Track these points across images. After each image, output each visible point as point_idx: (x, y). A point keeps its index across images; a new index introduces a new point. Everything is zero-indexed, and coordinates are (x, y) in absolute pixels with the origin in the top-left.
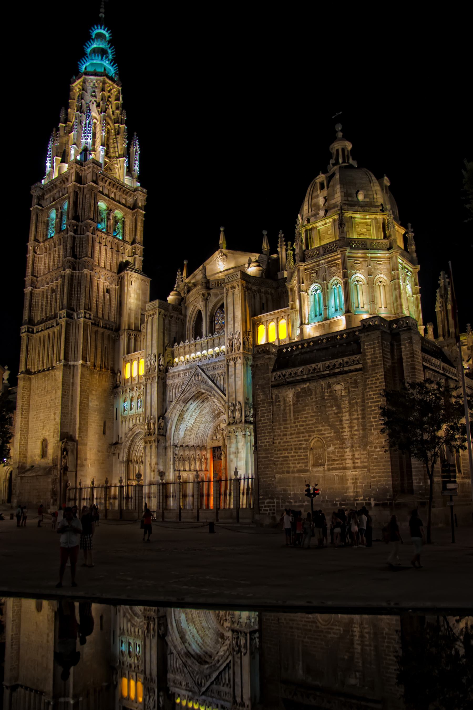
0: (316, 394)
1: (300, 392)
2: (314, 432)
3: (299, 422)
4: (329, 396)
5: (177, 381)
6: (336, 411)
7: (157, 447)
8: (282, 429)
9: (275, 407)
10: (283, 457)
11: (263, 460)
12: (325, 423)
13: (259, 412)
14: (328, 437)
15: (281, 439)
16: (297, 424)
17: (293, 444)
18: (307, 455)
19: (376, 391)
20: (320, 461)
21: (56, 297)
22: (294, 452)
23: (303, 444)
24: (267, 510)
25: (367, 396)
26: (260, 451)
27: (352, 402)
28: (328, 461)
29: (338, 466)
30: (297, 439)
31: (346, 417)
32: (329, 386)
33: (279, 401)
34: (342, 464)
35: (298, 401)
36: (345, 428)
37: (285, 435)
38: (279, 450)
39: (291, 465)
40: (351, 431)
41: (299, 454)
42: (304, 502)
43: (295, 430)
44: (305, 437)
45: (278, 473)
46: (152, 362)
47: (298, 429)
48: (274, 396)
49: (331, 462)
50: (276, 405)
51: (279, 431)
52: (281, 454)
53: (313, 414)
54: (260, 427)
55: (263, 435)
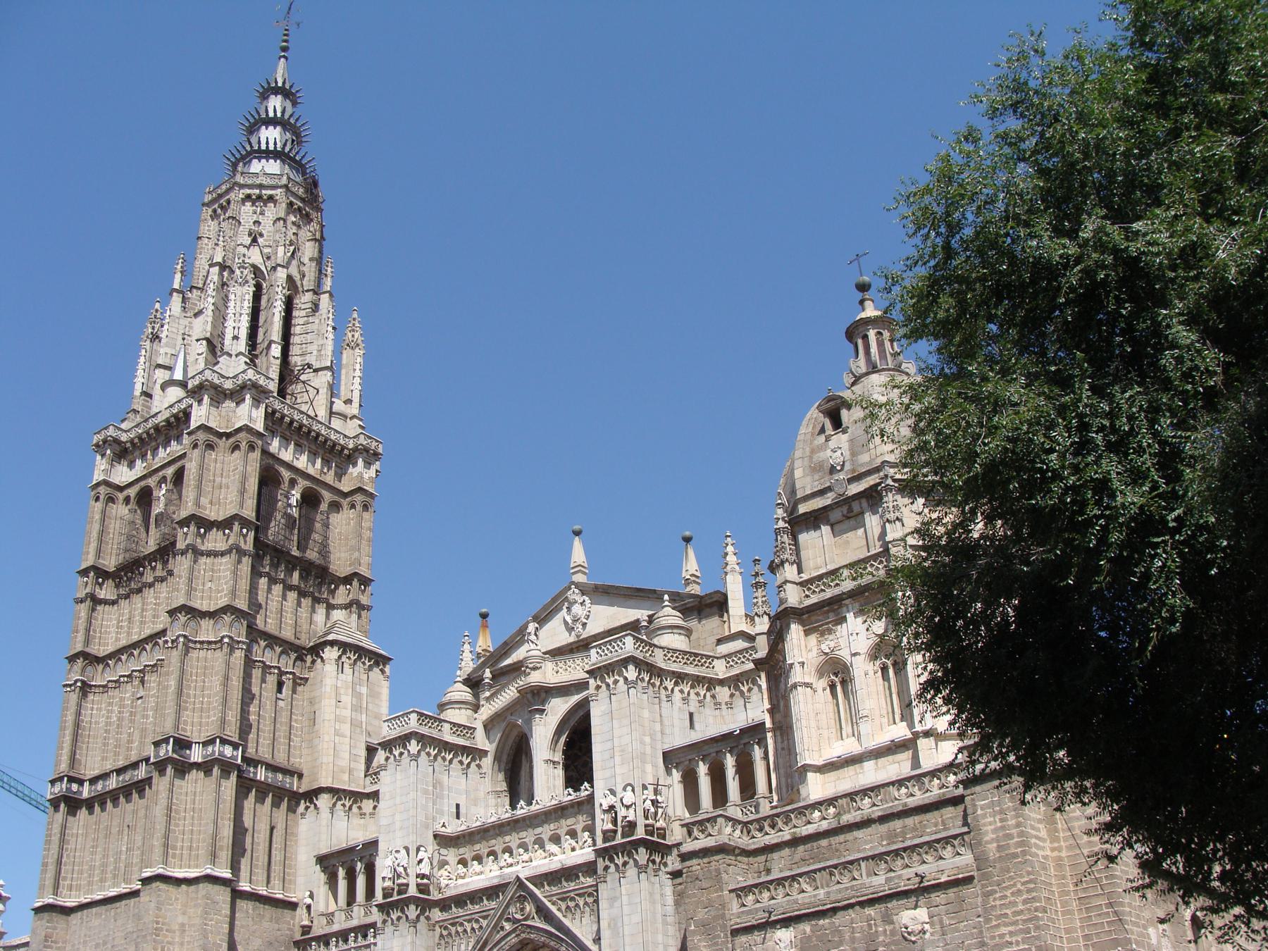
0: (853, 940)
19: (1015, 923)
25: (993, 938)
32: (887, 919)
46: (400, 870)
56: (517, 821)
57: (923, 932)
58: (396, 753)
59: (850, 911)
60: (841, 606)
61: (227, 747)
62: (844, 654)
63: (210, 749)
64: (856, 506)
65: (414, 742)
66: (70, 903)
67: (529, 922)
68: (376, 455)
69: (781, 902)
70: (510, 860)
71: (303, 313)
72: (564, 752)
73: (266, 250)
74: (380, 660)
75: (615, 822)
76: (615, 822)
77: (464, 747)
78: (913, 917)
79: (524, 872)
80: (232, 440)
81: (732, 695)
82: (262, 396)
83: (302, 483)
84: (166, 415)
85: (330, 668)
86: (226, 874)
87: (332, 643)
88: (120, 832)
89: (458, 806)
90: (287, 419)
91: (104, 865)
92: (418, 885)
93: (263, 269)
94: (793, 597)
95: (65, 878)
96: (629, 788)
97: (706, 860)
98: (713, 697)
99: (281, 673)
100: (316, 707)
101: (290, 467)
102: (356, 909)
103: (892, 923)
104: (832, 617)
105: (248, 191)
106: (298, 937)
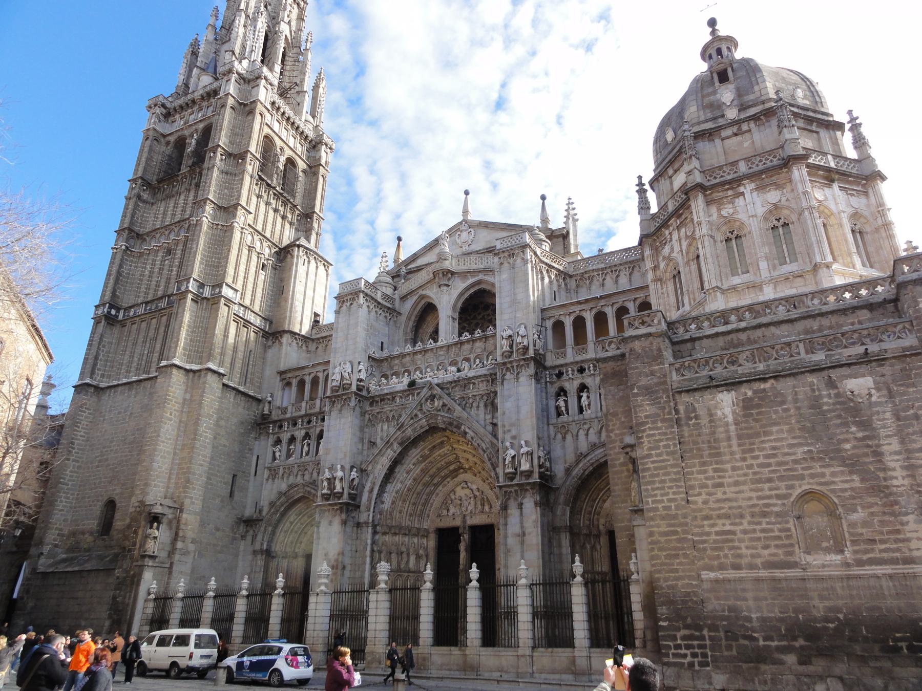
0: (796, 401)
1: (751, 399)
2: (802, 477)
3: (757, 457)
4: (834, 404)
5: (387, 408)
6: (860, 435)
7: (344, 523)
8: (711, 473)
9: (685, 428)
10: (717, 533)
11: (663, 539)
12: (831, 459)
13: (645, 439)
14: (845, 490)
15: (710, 494)
16: (750, 462)
17: (744, 504)
18: (789, 530)
20: (825, 544)
21: (172, 261)
22: (749, 523)
23: (775, 505)
24: (685, 656)
26: (652, 519)
27: (903, 414)
28: (854, 542)
29: (885, 555)
30: (754, 494)
31: (890, 446)
32: (831, 384)
33: (697, 417)
34: (898, 550)
35: (744, 416)
36: (894, 469)
37: (720, 485)
38: (707, 518)
39: (744, 551)
40: (913, 476)
41: (764, 526)
42: (795, 639)
43: (745, 475)
44: (777, 489)
45: (710, 569)
47: (755, 473)
48: (681, 408)
49: (863, 547)
50: (688, 425)
51: (702, 476)
52: (713, 526)
53: (795, 441)
54: (649, 469)
55: (657, 485)
56: (426, 351)
57: (870, 395)
58: (348, 304)
59: (792, 378)
60: (739, 186)
62: (742, 216)
63: (217, 291)
64: (745, 127)
65: (362, 295)
66: (103, 385)
69: (719, 371)
72: (460, 313)
73: (272, 14)
74: (327, 264)
76: (511, 346)
77: (389, 308)
78: (860, 384)
79: (436, 381)
80: (247, 108)
81: (577, 286)
83: (288, 153)
84: (201, 92)
86: (222, 371)
87: (299, 246)
90: (282, 110)
94: (698, 178)
95: (99, 370)
96: (523, 326)
97: (648, 342)
98: (566, 285)
102: (304, 404)
103: (836, 387)
104: (730, 193)
106: (260, 421)
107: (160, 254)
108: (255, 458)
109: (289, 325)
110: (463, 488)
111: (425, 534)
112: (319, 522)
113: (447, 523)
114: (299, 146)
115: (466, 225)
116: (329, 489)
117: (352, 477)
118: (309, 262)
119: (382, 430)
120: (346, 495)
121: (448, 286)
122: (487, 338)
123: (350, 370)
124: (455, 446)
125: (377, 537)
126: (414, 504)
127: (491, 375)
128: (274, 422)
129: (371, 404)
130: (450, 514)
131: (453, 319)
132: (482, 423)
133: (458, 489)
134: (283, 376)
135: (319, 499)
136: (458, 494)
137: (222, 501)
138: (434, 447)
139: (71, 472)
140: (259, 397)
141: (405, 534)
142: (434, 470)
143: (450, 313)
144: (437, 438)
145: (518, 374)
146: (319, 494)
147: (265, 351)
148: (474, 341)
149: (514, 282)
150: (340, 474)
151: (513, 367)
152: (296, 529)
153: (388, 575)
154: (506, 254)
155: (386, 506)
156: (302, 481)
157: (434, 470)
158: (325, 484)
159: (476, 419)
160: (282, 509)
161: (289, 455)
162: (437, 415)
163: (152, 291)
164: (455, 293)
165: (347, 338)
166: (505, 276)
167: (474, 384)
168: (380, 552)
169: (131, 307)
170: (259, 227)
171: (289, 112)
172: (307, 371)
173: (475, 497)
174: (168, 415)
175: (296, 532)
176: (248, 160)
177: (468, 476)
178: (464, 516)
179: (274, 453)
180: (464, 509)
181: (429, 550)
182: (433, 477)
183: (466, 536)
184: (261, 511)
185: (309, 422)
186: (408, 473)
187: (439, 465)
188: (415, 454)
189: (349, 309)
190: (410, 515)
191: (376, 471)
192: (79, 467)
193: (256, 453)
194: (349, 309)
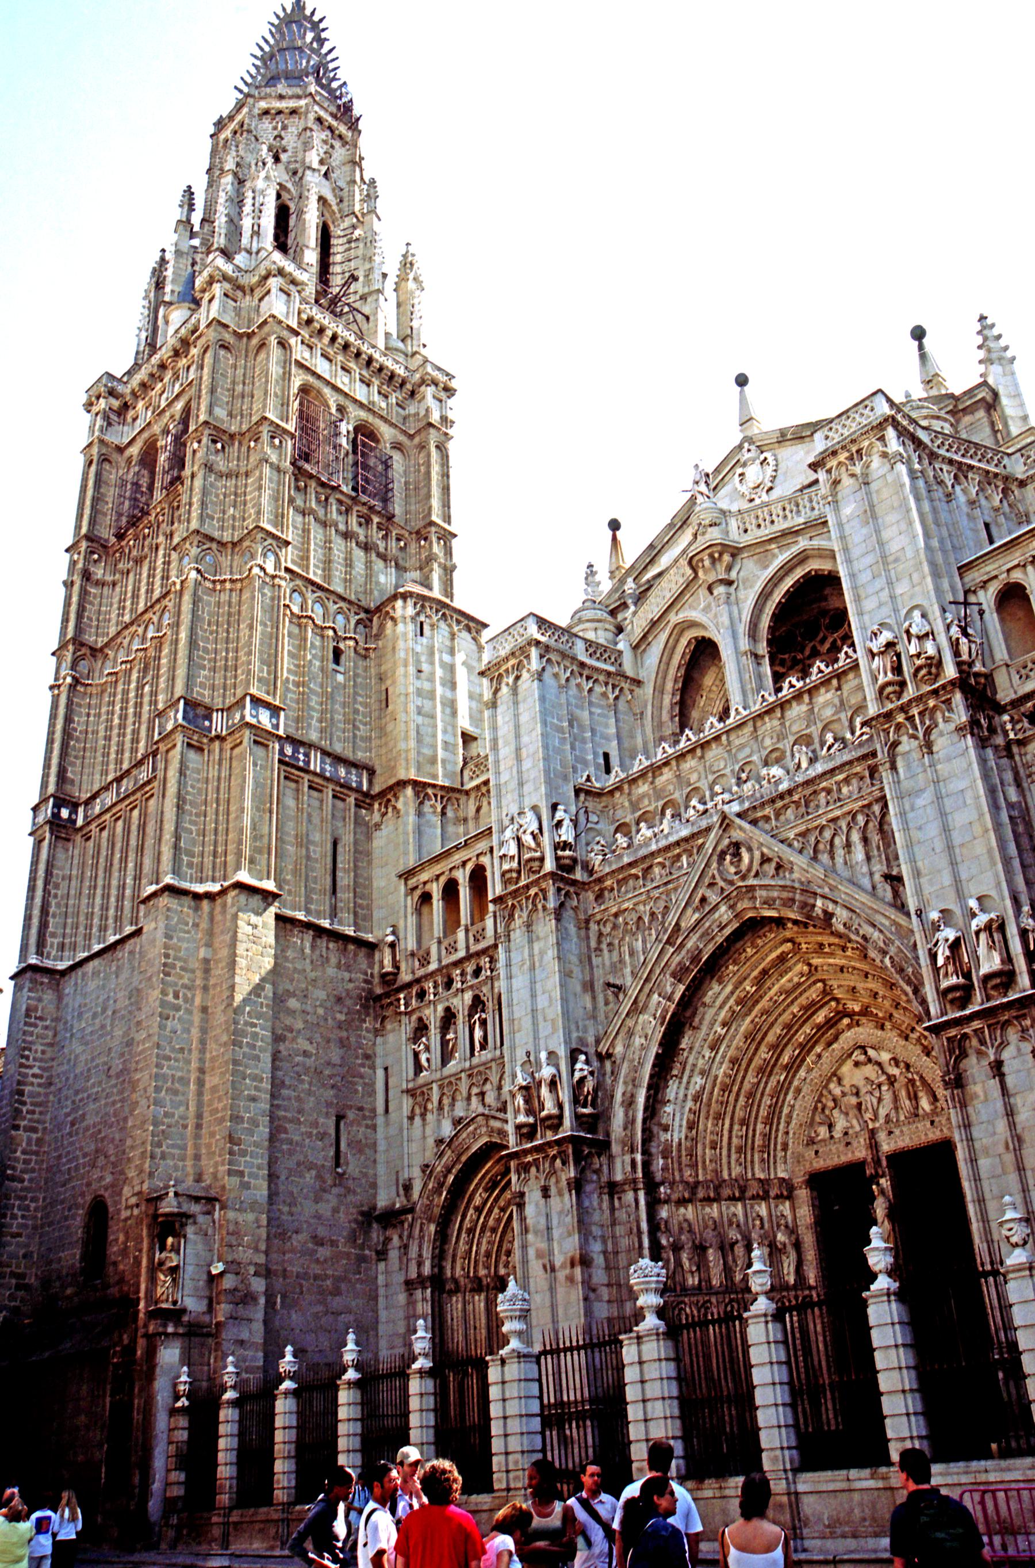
46: (528, 839)
58: (511, 680)
61: (261, 710)
66: (61, 966)
67: (751, 882)
68: (450, 391)
70: (701, 808)
71: (341, 241)
75: (898, 669)
76: (898, 669)
77: (609, 674)
82: (292, 287)
83: (355, 414)
85: (405, 629)
86: (269, 885)
87: (405, 596)
88: (124, 860)
89: (606, 756)
91: (105, 908)
92: (558, 859)
93: (289, 185)
95: (53, 935)
96: (917, 614)
99: (337, 638)
100: (389, 682)
101: (335, 388)
102: (461, 935)
105: (263, 104)
107: (135, 676)
108: (380, 1073)
109: (407, 769)
110: (857, 1064)
111: (788, 1191)
112: (522, 1195)
113: (835, 1157)
114: (376, 398)
115: (754, 445)
116: (529, 1112)
117: (577, 1075)
118: (432, 626)
119: (632, 954)
120: (567, 1122)
121: (729, 583)
122: (840, 676)
123: (534, 827)
124: (816, 961)
125: (664, 1213)
126: (744, 1122)
127: (864, 757)
128: (409, 985)
129: (599, 897)
130: (837, 1133)
131: (756, 656)
132: (866, 882)
133: (847, 1068)
134: (412, 882)
135: (512, 1140)
136: (846, 1082)
137: (319, 1177)
138: (765, 972)
139: (24, 1152)
140: (370, 938)
141: (732, 1198)
142: (777, 1030)
143: (744, 644)
144: (768, 949)
145: (928, 732)
146: (510, 1128)
147: (369, 838)
148: (811, 691)
149: (874, 517)
150: (547, 1072)
151: (910, 719)
152: (491, 1222)
153: (662, 1293)
154: (842, 457)
155: (677, 1134)
156: (481, 1109)
157: (777, 1030)
158: (520, 1100)
159: (847, 882)
160: (451, 1178)
161: (446, 1057)
162: (751, 888)
163: (127, 755)
164: (748, 598)
165: (519, 759)
166: (849, 509)
167: (829, 791)
168: (677, 1248)
169: (94, 797)
170: (315, 575)
171: (346, 335)
172: (457, 858)
173: (891, 1080)
174: (170, 998)
175: (494, 1230)
176: (265, 436)
177: (865, 1032)
178: (873, 1133)
179: (416, 1055)
180: (868, 1116)
181: (801, 1230)
182: (777, 1048)
183: (884, 1182)
184: (408, 1188)
185: (477, 973)
186: (714, 1047)
187: (786, 1017)
188: (719, 995)
189: (515, 690)
190: (740, 1150)
191: (634, 1054)
192: (39, 1142)
193: (379, 1062)
194: (515, 690)
